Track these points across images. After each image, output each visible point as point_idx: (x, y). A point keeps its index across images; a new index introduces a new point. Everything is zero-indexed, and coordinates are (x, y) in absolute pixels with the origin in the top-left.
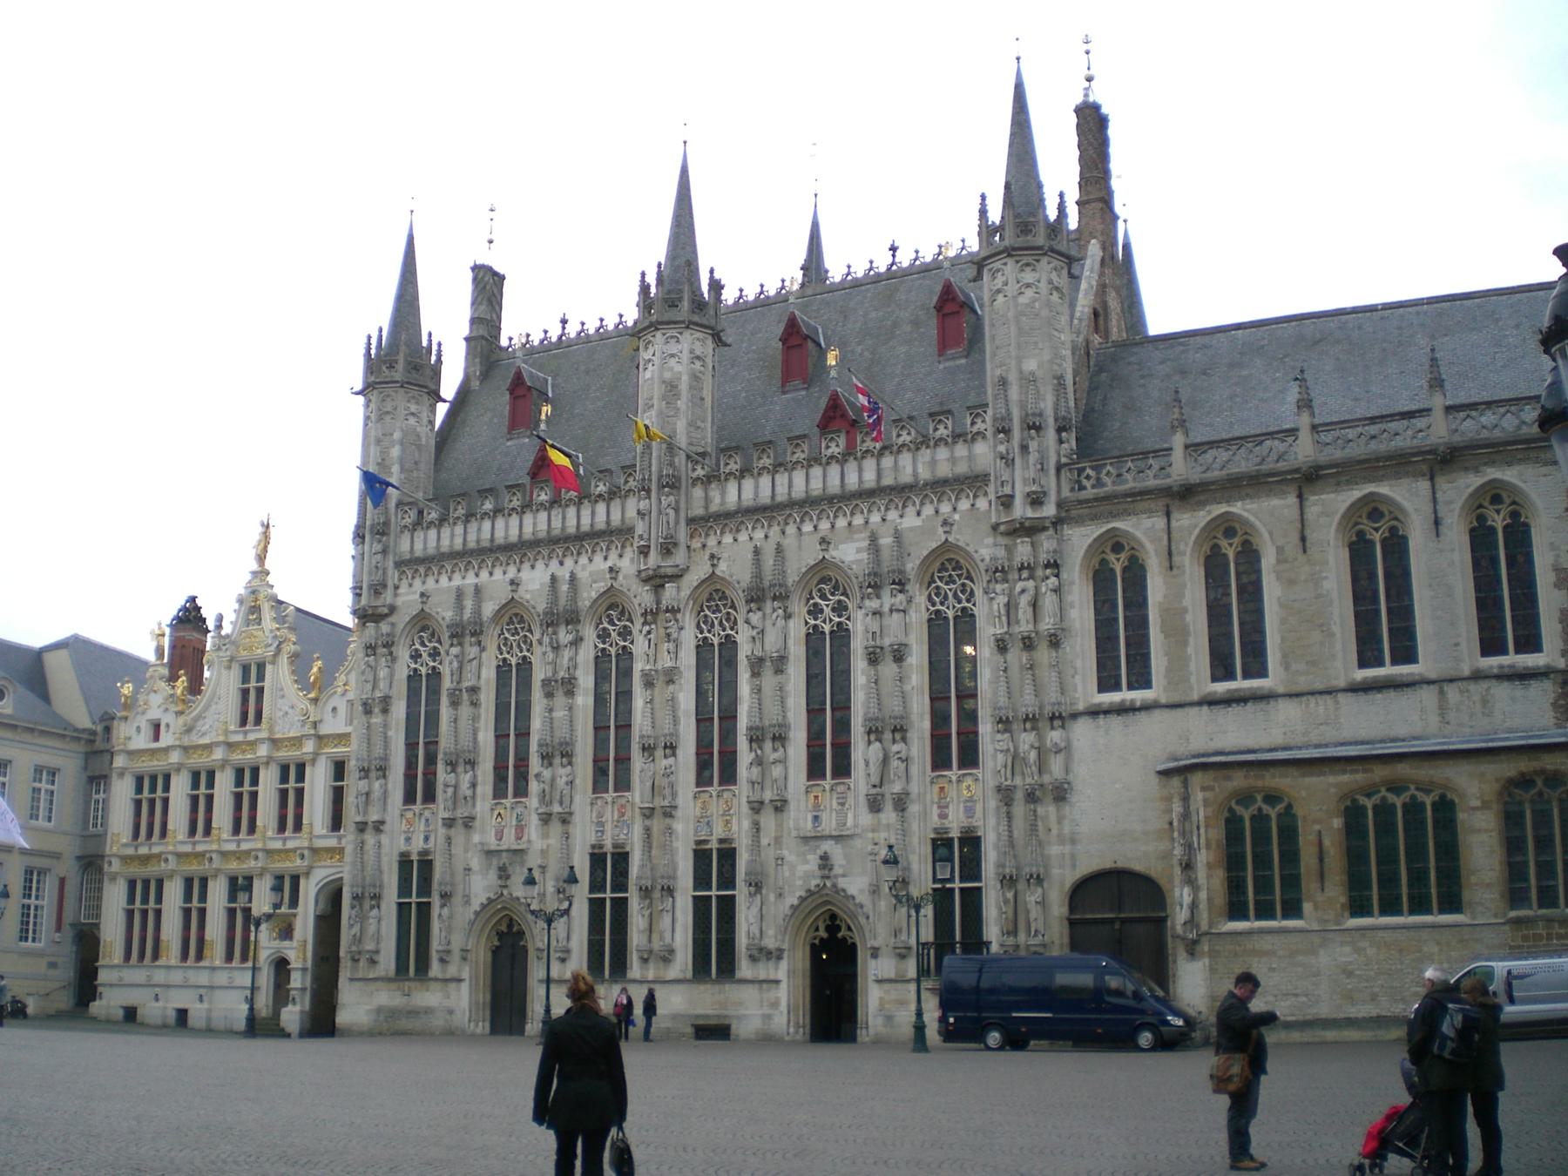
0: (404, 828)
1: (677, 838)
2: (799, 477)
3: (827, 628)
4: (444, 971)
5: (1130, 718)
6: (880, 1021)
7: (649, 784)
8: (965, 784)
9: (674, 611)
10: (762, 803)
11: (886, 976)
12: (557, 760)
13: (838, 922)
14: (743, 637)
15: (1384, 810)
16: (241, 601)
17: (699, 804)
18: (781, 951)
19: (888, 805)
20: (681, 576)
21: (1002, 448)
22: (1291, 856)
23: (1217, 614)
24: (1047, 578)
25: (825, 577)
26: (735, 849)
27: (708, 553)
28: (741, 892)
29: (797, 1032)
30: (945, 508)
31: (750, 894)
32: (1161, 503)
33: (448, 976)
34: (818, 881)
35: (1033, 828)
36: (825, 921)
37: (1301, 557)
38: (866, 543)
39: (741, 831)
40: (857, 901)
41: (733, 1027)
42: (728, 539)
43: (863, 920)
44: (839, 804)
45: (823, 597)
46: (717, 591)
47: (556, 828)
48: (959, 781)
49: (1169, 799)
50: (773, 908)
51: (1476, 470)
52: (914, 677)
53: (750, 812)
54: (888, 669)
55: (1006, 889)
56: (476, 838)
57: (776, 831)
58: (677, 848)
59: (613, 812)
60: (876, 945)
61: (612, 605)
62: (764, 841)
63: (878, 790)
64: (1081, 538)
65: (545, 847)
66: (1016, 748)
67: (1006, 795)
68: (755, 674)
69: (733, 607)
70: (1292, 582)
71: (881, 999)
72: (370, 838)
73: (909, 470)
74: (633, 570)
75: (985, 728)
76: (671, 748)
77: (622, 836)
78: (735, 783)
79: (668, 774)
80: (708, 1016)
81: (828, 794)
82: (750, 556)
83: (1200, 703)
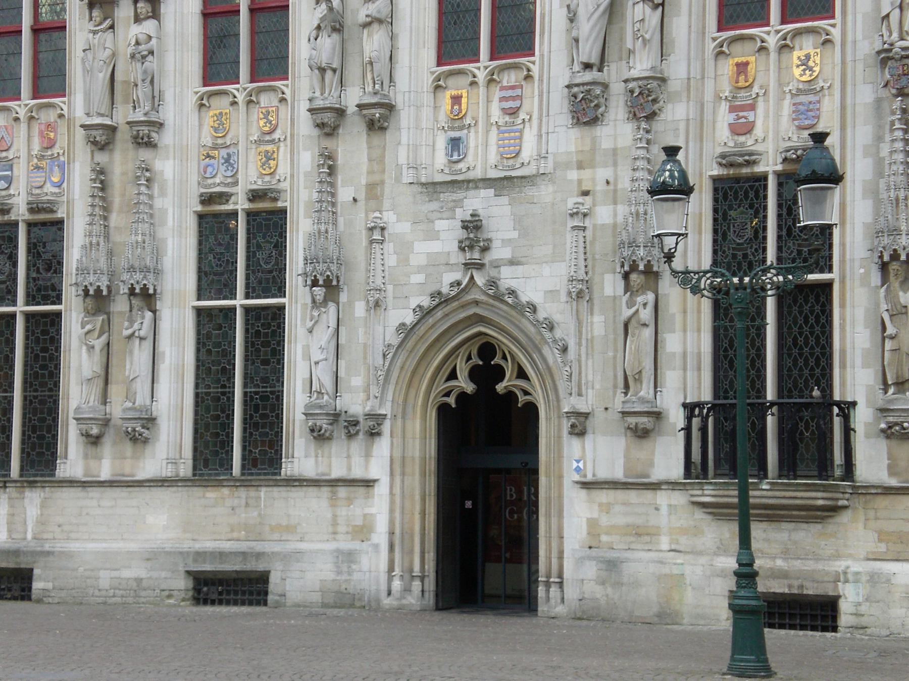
1: (163, 194)
6: (591, 571)
7: (102, 77)
8: (796, 54)
10: (341, 112)
11: (603, 474)
13: (497, 360)
17: (209, 119)
18: (378, 419)
26: (284, 211)
29: (407, 590)
31: (314, 301)
34: (456, 276)
36: (469, 358)
40: (541, 315)
41: (274, 579)
43: (552, 355)
44: (505, 111)
48: (784, 47)
50: (361, 331)
53: (316, 132)
55: (895, 284)
57: (370, 172)
58: (164, 211)
59: (29, 137)
60: (583, 408)
62: (345, 194)
63: (588, 76)
71: (592, 524)
77: (49, 188)
80: (222, 555)
81: (482, 90)
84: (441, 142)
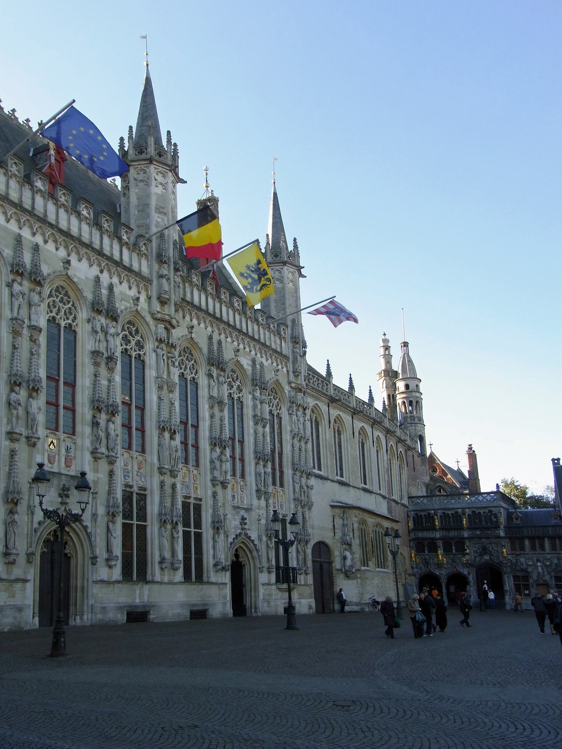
4: (9, 573)
33: (13, 577)
47: (104, 466)
65: (96, 479)
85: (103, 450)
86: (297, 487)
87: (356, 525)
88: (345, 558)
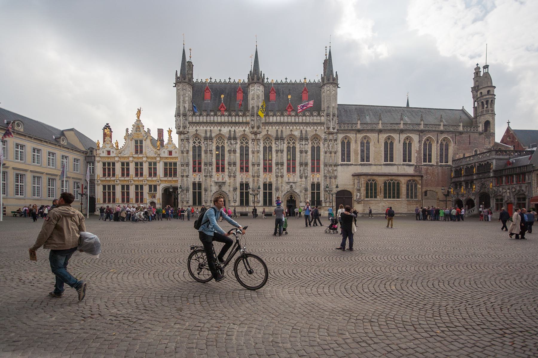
0: (193, 177)
2: (286, 118)
3: (291, 146)
5: (348, 166)
9: (259, 140)
12: (232, 166)
14: (274, 146)
15: (390, 183)
16: (133, 126)
17: (264, 175)
19: (304, 178)
20: (260, 133)
21: (329, 119)
22: (375, 189)
23: (362, 151)
24: (334, 142)
25: (291, 137)
26: (272, 184)
27: (266, 130)
28: (274, 191)
30: (316, 128)
32: (355, 132)
35: (330, 183)
37: (378, 144)
38: (300, 132)
39: (273, 180)
42: (270, 128)
45: (290, 141)
46: (268, 137)
47: (232, 178)
49: (354, 179)
51: (406, 134)
52: (309, 156)
54: (304, 154)
56: (213, 180)
61: (244, 137)
62: (279, 183)
64: (340, 136)
66: (329, 169)
67: (325, 176)
68: (277, 153)
69: (271, 140)
70: (376, 148)
72: (185, 179)
73: (308, 120)
74: (249, 131)
75: (322, 166)
76: (259, 165)
78: (272, 172)
79: (258, 169)
82: (275, 132)
83: (360, 165)
84: (287, 179)
85: (232, 175)
86: (326, 171)
87: (363, 182)
88: (357, 196)
